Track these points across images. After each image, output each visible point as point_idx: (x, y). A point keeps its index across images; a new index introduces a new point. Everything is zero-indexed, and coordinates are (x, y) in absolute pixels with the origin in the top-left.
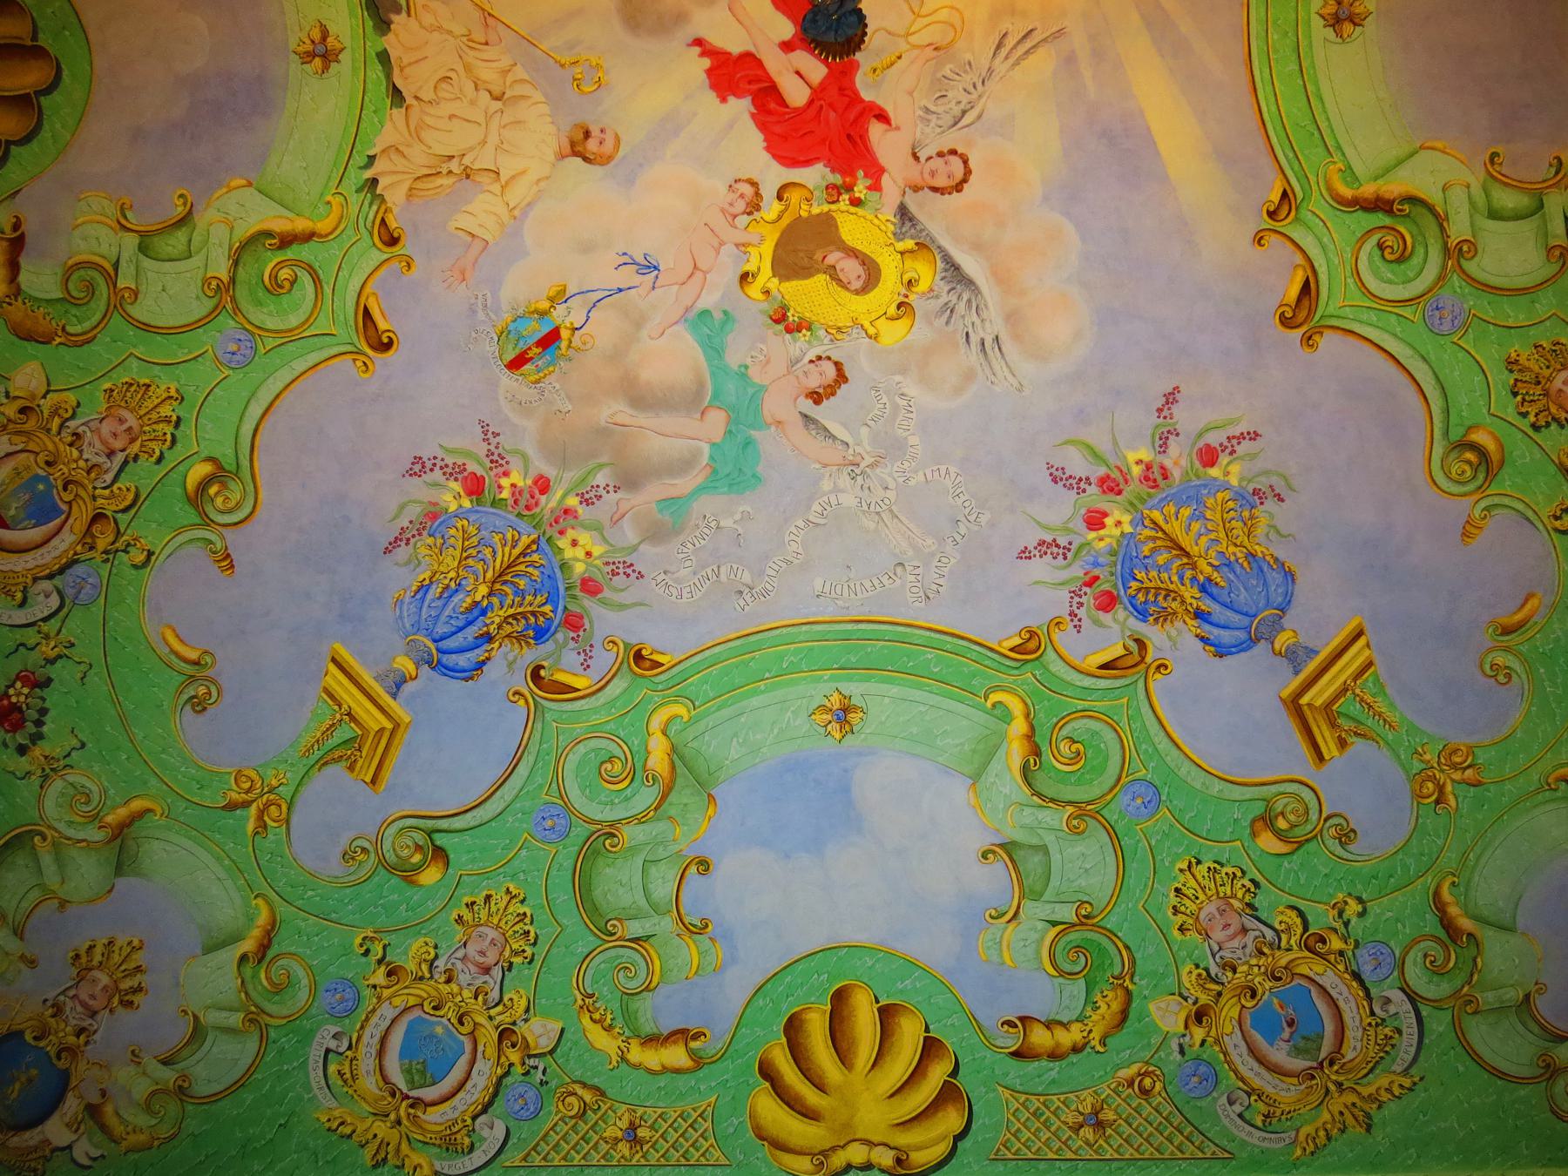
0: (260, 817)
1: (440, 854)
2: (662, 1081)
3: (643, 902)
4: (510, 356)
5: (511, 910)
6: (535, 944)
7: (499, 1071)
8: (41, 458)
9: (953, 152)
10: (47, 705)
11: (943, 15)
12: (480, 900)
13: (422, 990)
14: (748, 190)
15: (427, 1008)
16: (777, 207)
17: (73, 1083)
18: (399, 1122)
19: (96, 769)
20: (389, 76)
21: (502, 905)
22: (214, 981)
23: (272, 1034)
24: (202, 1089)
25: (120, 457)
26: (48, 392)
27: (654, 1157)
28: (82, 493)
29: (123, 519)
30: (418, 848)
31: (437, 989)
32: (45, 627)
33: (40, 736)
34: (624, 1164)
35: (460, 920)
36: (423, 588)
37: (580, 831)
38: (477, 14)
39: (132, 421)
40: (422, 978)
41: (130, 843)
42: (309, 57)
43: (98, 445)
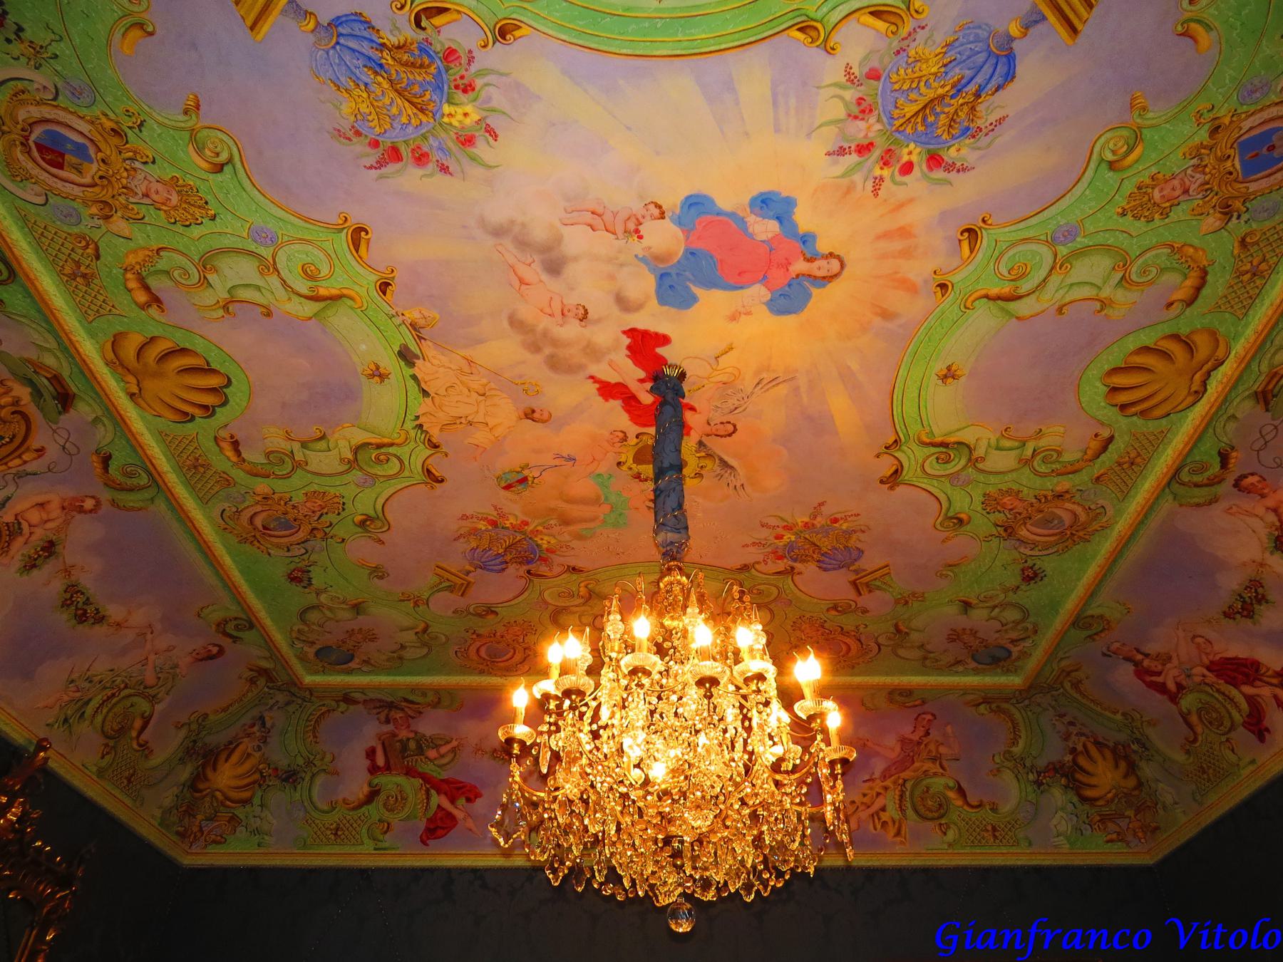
4: (503, 484)
14: (621, 435)
16: (635, 441)
20: (419, 385)
25: (318, 514)
37: (551, 608)
38: (465, 361)
42: (373, 376)
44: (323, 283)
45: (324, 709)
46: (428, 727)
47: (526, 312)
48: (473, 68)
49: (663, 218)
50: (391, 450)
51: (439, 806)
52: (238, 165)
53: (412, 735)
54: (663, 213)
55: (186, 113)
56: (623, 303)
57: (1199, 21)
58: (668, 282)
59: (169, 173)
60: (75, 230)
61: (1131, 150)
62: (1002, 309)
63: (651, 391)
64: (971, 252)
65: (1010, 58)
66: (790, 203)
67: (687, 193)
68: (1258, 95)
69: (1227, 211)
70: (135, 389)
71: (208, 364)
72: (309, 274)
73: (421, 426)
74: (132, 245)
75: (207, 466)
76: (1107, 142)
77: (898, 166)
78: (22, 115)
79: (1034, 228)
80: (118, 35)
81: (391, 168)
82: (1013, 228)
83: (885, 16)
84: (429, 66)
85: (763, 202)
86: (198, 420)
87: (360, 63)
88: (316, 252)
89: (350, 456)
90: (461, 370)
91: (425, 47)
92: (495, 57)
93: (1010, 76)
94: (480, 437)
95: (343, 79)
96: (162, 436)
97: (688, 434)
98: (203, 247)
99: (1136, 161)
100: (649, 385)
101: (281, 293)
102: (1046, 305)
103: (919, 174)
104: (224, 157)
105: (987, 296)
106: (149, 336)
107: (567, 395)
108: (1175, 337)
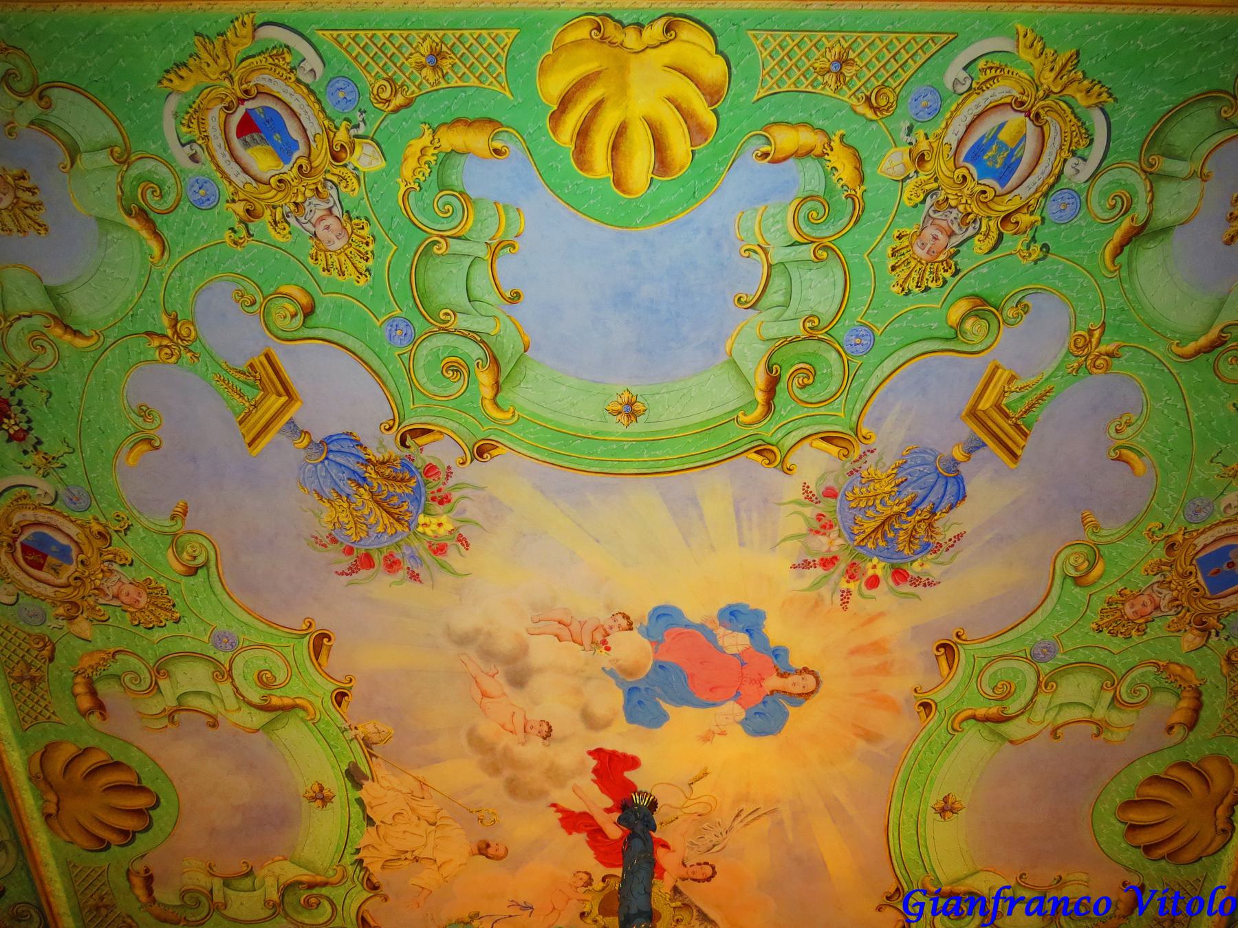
9: (706, 863)
11: (705, 799)
14: (586, 877)
16: (602, 885)
20: (364, 810)
38: (416, 783)
42: (314, 799)
44: (278, 692)
47: (487, 729)
48: (451, 482)
49: (631, 629)
50: (324, 891)
52: (213, 569)
54: (631, 624)
55: (173, 518)
56: (590, 721)
57: (1129, 448)
58: (636, 697)
59: (142, 574)
60: (37, 630)
61: (1092, 566)
62: (992, 732)
63: (619, 822)
64: (951, 668)
65: (959, 481)
66: (759, 615)
67: (655, 605)
68: (1203, 514)
69: (1203, 628)
70: (52, 810)
71: (139, 781)
72: (264, 681)
73: (360, 861)
74: (90, 647)
75: (110, 908)
76: (1068, 558)
77: (864, 579)
78: (17, 518)
79: (1008, 643)
80: (126, 449)
81: (363, 573)
82: (989, 643)
83: (835, 441)
84: (409, 480)
85: (732, 614)
86: (114, 848)
87: (345, 476)
88: (275, 658)
89: (275, 897)
90: (412, 793)
91: (407, 464)
92: (475, 472)
93: (961, 496)
94: (426, 877)
95: (326, 490)
96: (68, 868)
97: (661, 877)
98: (160, 651)
99: (1100, 577)
100: (616, 816)
101: (231, 702)
102: (1039, 728)
103: (886, 589)
104: (200, 560)
105: (974, 717)
106: (83, 747)
107: (530, 827)
108: (1184, 765)
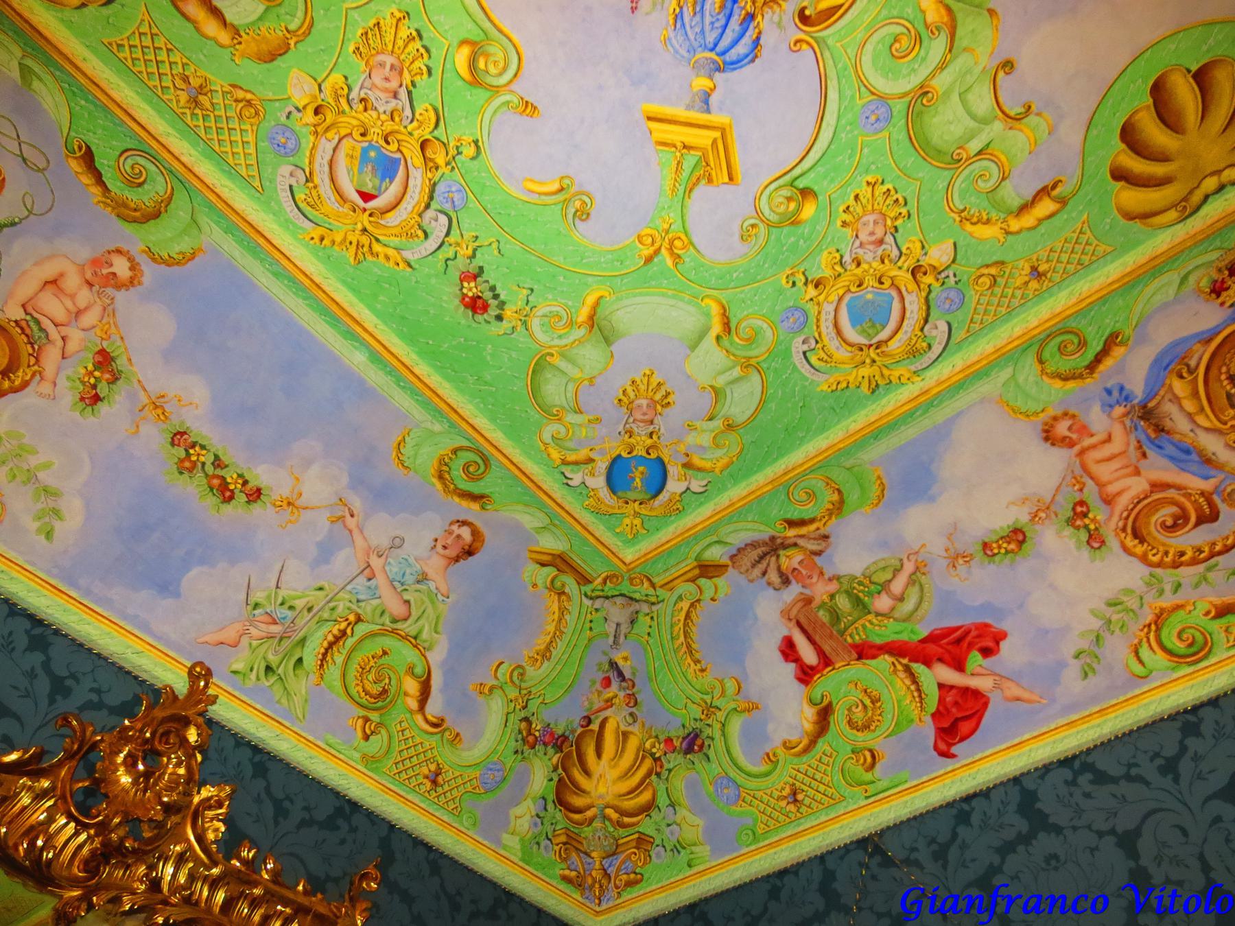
0: (672, 253)
1: (806, 193)
2: (1042, 229)
3: (972, 124)
5: (877, 193)
6: (906, 204)
7: (924, 294)
8: (356, 135)
10: (492, 283)
12: (851, 201)
13: (842, 282)
15: (853, 289)
17: (666, 460)
18: (874, 361)
19: (550, 297)
21: (869, 195)
22: (708, 363)
23: (765, 366)
24: (741, 419)
25: (403, 94)
26: (320, 86)
27: (1057, 278)
28: (400, 137)
29: (440, 132)
30: (789, 199)
31: (855, 275)
32: (451, 239)
33: (503, 303)
34: (1038, 295)
35: (844, 224)
36: (678, 17)
37: (899, 107)
39: (389, 60)
40: (839, 275)
41: (604, 323)
43: (382, 95)
45: (685, 605)
46: (851, 555)
51: (941, 686)
53: (833, 587)
